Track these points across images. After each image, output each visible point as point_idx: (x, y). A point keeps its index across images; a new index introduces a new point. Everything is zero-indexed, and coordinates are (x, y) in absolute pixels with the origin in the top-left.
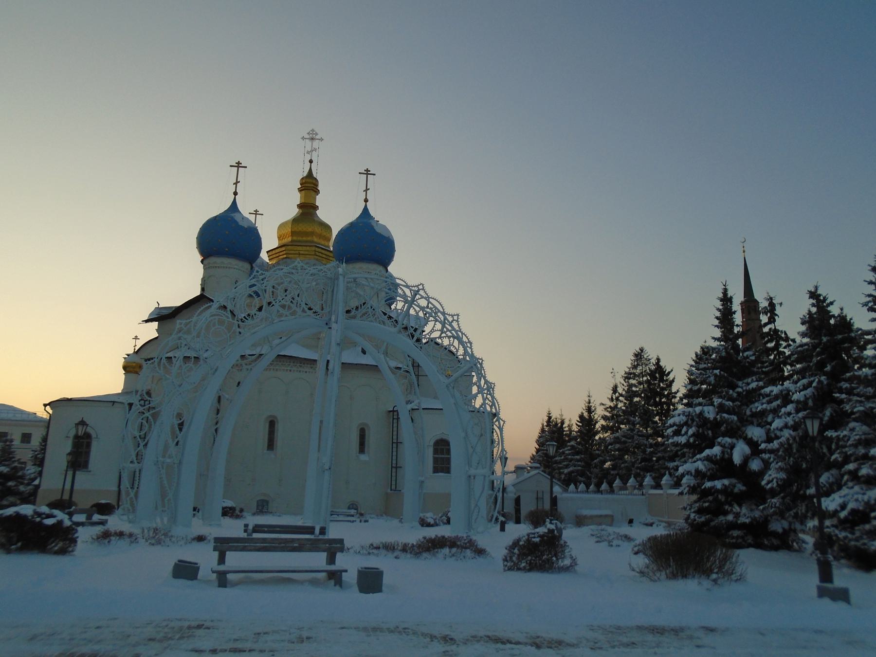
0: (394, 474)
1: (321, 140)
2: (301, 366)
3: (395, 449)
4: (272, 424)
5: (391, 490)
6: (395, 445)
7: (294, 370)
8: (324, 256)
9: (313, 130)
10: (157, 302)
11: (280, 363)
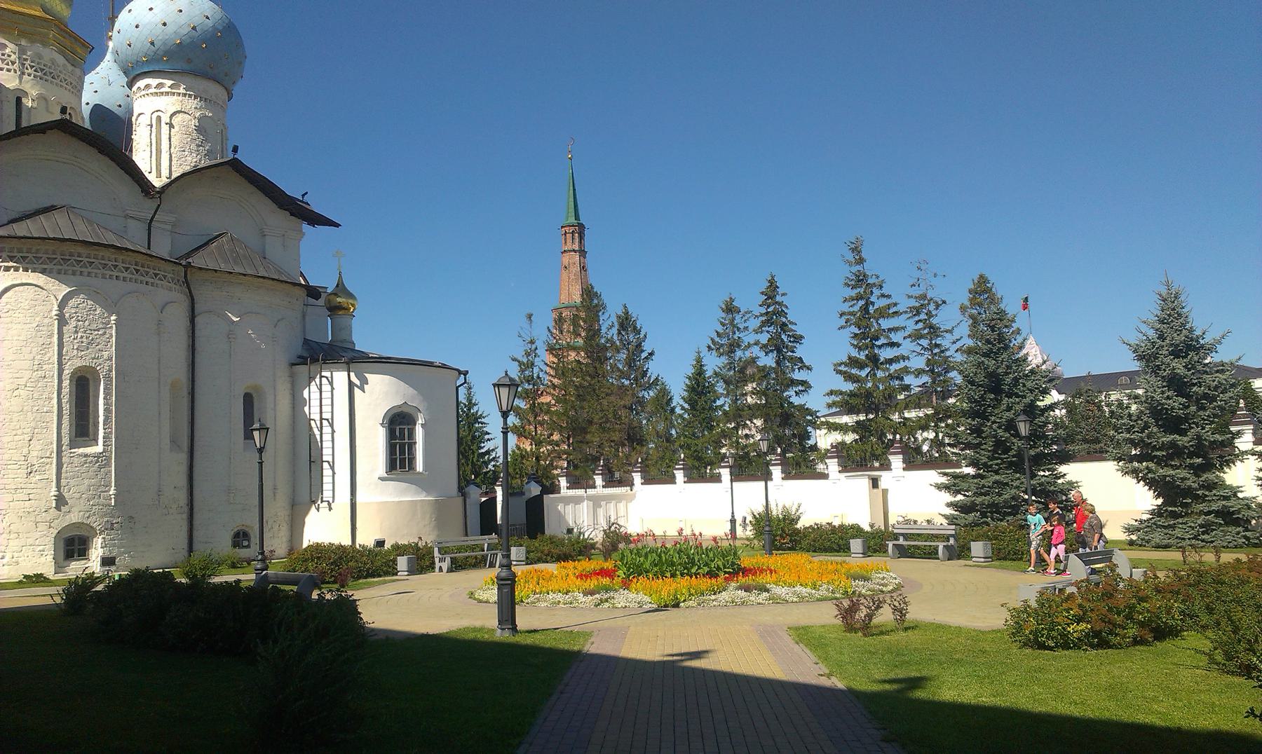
2: (137, 271)
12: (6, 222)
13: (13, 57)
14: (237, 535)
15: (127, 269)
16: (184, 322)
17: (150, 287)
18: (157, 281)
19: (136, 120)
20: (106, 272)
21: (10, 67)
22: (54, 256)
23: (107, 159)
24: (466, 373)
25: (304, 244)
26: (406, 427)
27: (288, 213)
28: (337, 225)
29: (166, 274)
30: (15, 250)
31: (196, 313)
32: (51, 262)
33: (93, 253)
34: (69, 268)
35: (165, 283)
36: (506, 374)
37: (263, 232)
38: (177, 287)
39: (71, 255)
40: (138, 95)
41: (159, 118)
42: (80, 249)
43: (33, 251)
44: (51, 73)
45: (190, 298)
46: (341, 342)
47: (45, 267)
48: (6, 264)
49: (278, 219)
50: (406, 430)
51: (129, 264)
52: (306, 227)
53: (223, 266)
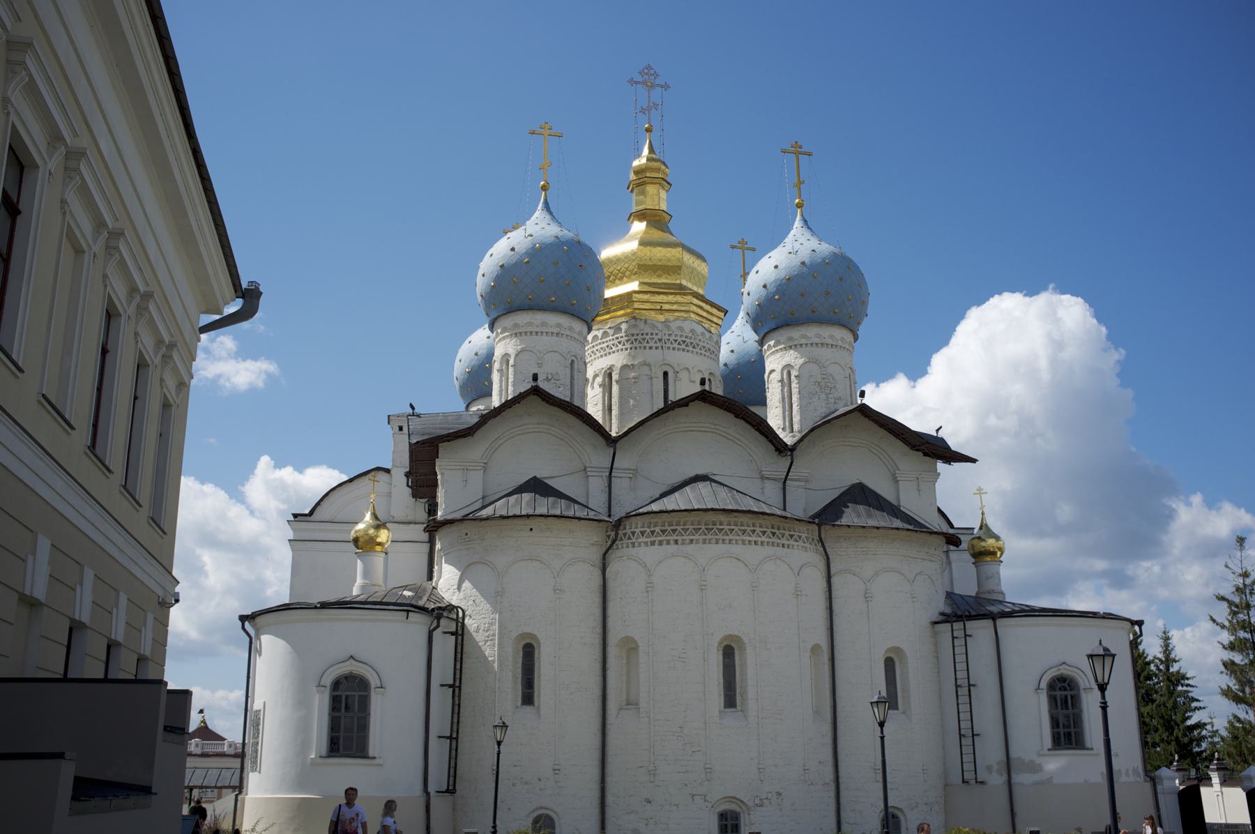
1: (666, 87)
2: (774, 534)
3: (964, 699)
4: (729, 653)
5: (976, 782)
7: (762, 542)
8: (705, 314)
9: (649, 67)
12: (658, 496)
15: (764, 533)
16: (821, 583)
17: (786, 550)
18: (792, 542)
19: (769, 377)
20: (745, 538)
22: (700, 527)
23: (742, 422)
24: (1140, 623)
25: (939, 485)
26: (1069, 693)
27: (920, 454)
28: (974, 461)
29: (801, 534)
30: (667, 524)
31: (832, 573)
32: (697, 533)
33: (733, 520)
34: (713, 537)
35: (800, 543)
36: (1101, 644)
37: (896, 477)
38: (812, 547)
39: (714, 524)
40: (768, 353)
42: (722, 518)
43: (682, 523)
44: (691, 343)
45: (825, 557)
46: (989, 592)
47: (692, 537)
48: (660, 538)
49: (909, 462)
51: (766, 528)
52: (941, 466)
53: (856, 520)
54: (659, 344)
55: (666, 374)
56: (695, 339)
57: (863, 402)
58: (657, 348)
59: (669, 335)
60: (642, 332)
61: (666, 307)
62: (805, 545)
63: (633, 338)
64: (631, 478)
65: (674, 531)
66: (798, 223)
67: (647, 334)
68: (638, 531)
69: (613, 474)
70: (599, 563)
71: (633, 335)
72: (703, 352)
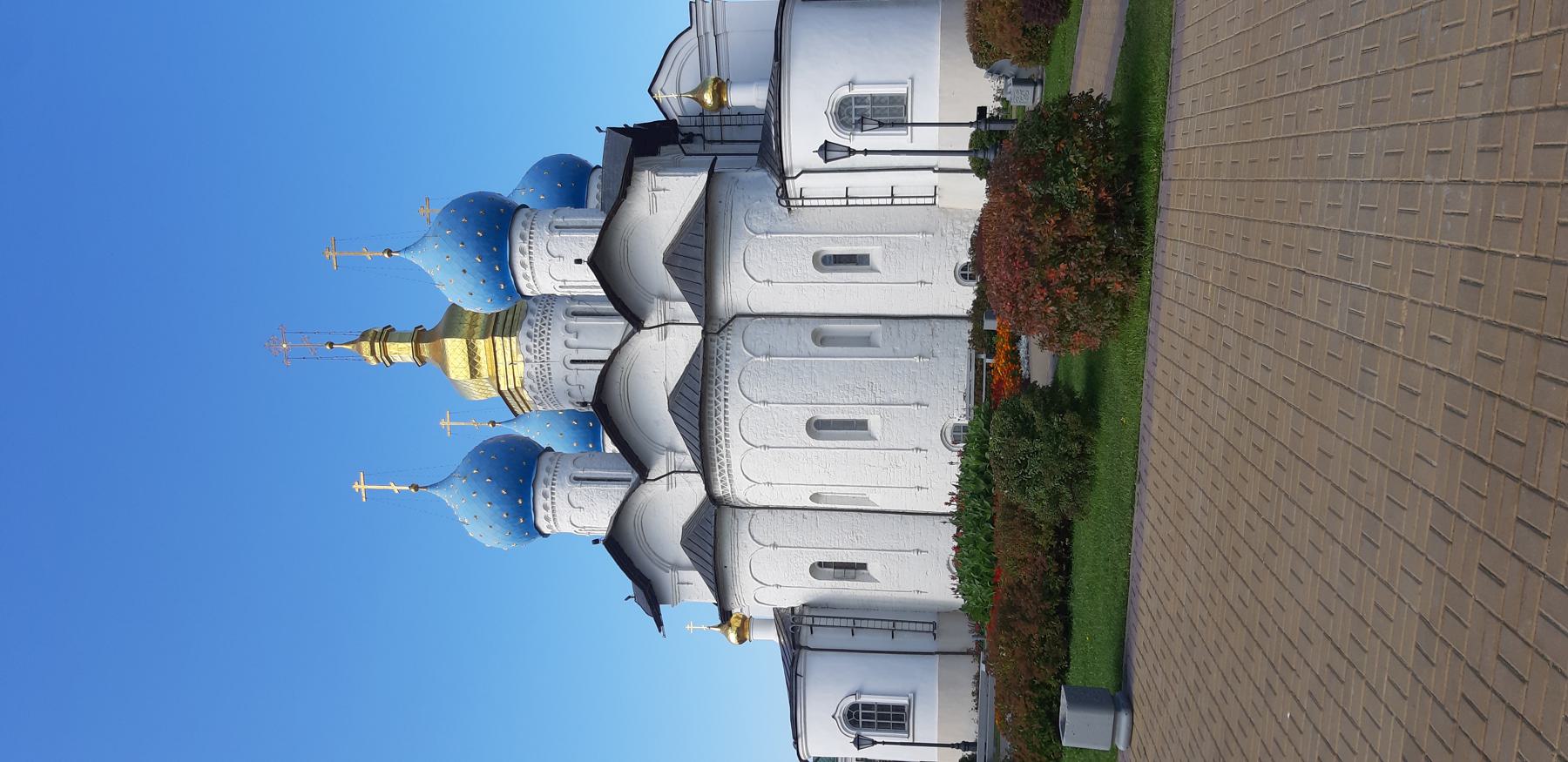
0: (906, 201)
3: (859, 202)
6: (851, 202)
10: (626, 599)
11: (715, 419)
13: (536, 365)
14: (964, 276)
18: (723, 363)
21: (546, 367)
27: (630, 189)
35: (722, 352)
41: (560, 287)
44: (540, 335)
47: (725, 455)
50: (856, 107)
54: (546, 367)
55: (573, 362)
56: (536, 331)
57: (586, 260)
58: (549, 369)
59: (535, 357)
60: (535, 380)
61: (509, 360)
62: (725, 344)
63: (542, 389)
64: (675, 452)
65: (719, 467)
66: (408, 256)
67: (537, 377)
68: (721, 491)
69: (673, 470)
70: (751, 511)
71: (539, 388)
72: (546, 321)
